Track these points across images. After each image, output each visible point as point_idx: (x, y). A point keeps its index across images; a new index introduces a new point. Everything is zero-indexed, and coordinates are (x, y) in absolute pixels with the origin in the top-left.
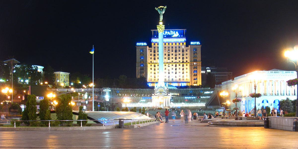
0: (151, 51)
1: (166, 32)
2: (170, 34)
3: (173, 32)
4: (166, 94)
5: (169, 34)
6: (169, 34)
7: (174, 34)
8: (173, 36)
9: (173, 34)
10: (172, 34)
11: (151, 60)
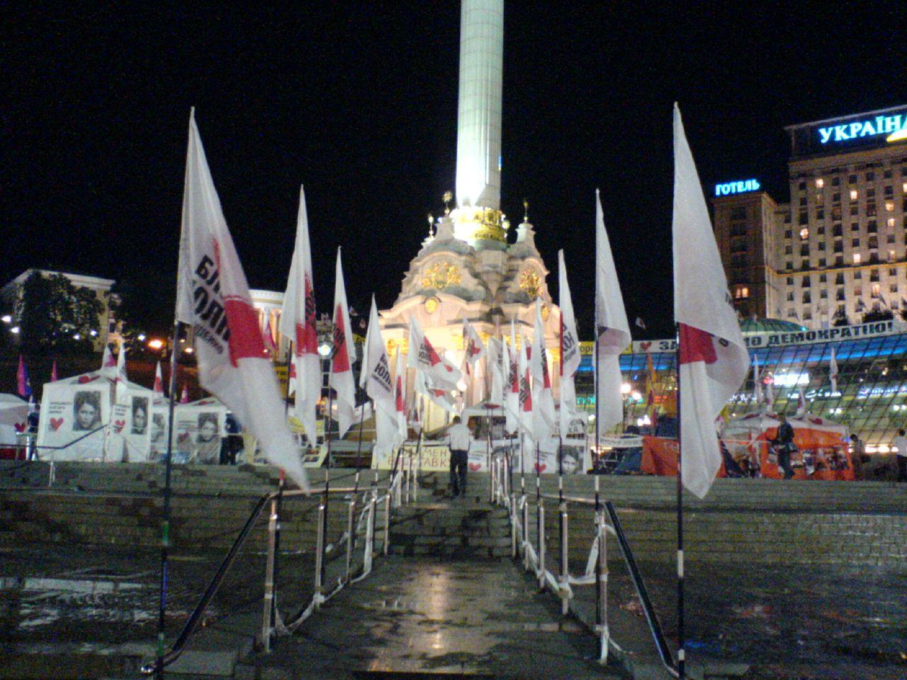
0: (788, 220)
1: (853, 126)
2: (872, 132)
3: (888, 119)
4: (476, 308)
5: (867, 134)
6: (867, 134)
7: (893, 127)
8: (889, 139)
9: (888, 129)
10: (884, 128)
11: (787, 258)
